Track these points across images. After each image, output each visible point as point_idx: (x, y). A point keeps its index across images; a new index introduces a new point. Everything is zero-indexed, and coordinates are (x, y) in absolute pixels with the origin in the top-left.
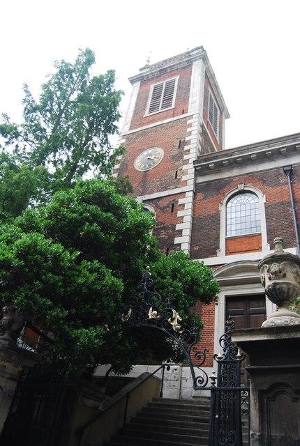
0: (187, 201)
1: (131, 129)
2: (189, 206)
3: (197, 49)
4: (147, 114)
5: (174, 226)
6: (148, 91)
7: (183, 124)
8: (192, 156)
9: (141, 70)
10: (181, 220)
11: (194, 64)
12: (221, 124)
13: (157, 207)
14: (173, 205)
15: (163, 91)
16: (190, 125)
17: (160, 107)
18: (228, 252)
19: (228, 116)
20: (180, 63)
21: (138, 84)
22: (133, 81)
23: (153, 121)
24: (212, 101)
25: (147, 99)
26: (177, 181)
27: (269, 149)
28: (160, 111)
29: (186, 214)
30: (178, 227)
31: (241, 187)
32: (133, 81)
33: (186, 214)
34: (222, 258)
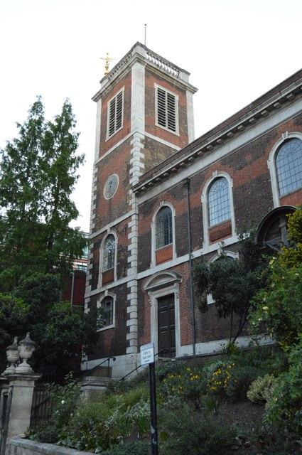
0: (133, 224)
1: (100, 157)
3: (135, 46)
4: (108, 138)
7: (128, 146)
9: (101, 82)
10: (129, 242)
11: (133, 68)
12: (183, 109)
13: (118, 232)
15: (116, 104)
17: (115, 128)
19: (194, 90)
21: (100, 101)
23: (112, 146)
24: (161, 93)
26: (128, 208)
28: (116, 132)
29: (133, 236)
30: (130, 248)
31: (162, 204)
32: (95, 99)
33: (133, 236)
34: (154, 269)
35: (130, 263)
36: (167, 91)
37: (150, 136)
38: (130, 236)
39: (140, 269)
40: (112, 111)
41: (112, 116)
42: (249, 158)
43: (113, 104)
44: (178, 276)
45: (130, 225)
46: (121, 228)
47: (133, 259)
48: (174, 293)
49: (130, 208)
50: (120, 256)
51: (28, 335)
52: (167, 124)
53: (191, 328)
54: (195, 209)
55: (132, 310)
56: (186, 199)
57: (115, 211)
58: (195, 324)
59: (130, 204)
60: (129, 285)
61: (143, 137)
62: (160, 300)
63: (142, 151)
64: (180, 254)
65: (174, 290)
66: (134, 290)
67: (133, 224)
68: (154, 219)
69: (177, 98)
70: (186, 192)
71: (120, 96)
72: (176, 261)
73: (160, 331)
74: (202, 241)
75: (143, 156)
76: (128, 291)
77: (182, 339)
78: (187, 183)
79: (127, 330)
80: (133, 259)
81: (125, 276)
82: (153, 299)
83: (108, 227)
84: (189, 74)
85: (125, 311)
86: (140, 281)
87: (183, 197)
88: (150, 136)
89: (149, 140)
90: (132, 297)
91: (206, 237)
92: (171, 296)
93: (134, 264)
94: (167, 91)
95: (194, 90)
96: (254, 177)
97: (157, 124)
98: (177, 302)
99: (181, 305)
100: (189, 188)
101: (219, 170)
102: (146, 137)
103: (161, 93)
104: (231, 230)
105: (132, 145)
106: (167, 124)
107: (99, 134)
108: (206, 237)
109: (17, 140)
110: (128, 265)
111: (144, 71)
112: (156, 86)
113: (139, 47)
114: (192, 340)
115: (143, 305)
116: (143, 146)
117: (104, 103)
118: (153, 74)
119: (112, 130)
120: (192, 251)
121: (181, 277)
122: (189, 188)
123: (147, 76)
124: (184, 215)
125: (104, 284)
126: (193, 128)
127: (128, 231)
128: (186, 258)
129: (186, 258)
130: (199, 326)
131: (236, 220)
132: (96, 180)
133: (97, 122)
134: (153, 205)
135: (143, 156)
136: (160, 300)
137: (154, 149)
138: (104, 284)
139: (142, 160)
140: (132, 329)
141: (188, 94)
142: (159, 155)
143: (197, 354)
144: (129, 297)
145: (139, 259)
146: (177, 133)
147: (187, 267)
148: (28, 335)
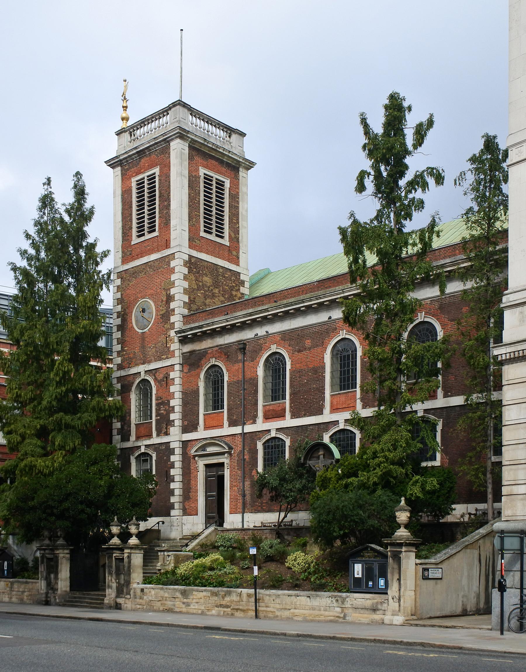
0: (175, 375)
2: (177, 381)
5: (169, 402)
6: (130, 190)
8: (176, 320)
10: (172, 396)
12: (235, 198)
13: (156, 380)
14: (167, 378)
16: (172, 271)
18: (206, 428)
19: (249, 165)
20: (156, 143)
21: (119, 169)
22: (112, 163)
23: (141, 255)
25: (131, 207)
26: (167, 353)
27: (228, 323)
29: (176, 389)
30: (172, 403)
31: (213, 362)
32: (112, 163)
33: (176, 389)
34: (201, 433)
35: (173, 421)
36: (216, 176)
37: (195, 253)
38: (172, 389)
39: (185, 430)
40: (141, 196)
41: (141, 206)
42: (308, 343)
43: (140, 184)
44: (230, 448)
45: (172, 375)
46: (160, 376)
47: (176, 416)
48: (224, 463)
49: (172, 354)
50: (160, 410)
51: (134, 518)
52: (214, 231)
53: (240, 498)
54: (250, 379)
55: (176, 472)
56: (241, 365)
57: (151, 351)
58: (244, 496)
59: (172, 349)
60: (172, 446)
61: (186, 258)
62: (207, 466)
63: (185, 278)
64: (233, 423)
65: (225, 460)
66: (178, 451)
67: (175, 375)
68: (202, 376)
69: (227, 184)
70: (240, 357)
71: (152, 178)
72: (227, 430)
73: (207, 497)
74: (256, 416)
75: (186, 284)
76: (172, 452)
77: (231, 508)
78: (242, 346)
79: (172, 492)
80: (176, 416)
81: (167, 434)
82: (201, 464)
83: (141, 369)
84: (243, 135)
85: (167, 473)
86: (185, 444)
87: (237, 361)
88: (195, 253)
89: (193, 260)
90: (176, 458)
91: (260, 414)
92: (222, 465)
93: (177, 423)
94: (216, 176)
95: (249, 165)
96: (311, 366)
97: (203, 234)
98: (227, 473)
99: (231, 477)
100: (244, 354)
101: (279, 345)
102: (190, 257)
103: (208, 179)
104: (285, 412)
105: (174, 268)
106: (214, 231)
107: (120, 225)
108: (260, 414)
109: (26, 252)
110: (170, 423)
111: (187, 149)
112: (202, 171)
113: (179, 110)
114: (241, 510)
115: (189, 469)
116: (186, 271)
117: (125, 177)
118: (198, 151)
119: (141, 229)
120: (244, 424)
121: (232, 449)
122: (244, 354)
123: (191, 158)
124: (238, 382)
125: (138, 438)
126: (246, 228)
127: (170, 382)
128: (237, 430)
129: (237, 430)
130: (248, 498)
131: (290, 404)
132: (119, 295)
133: (115, 204)
134: (200, 359)
135: (186, 284)
136: (207, 466)
137: (198, 273)
138: (138, 438)
139: (186, 291)
140: (177, 492)
141: (242, 173)
142: (206, 279)
143: (245, 527)
144: (173, 458)
145: (185, 416)
146: (226, 242)
147: (239, 439)
148: (134, 518)
